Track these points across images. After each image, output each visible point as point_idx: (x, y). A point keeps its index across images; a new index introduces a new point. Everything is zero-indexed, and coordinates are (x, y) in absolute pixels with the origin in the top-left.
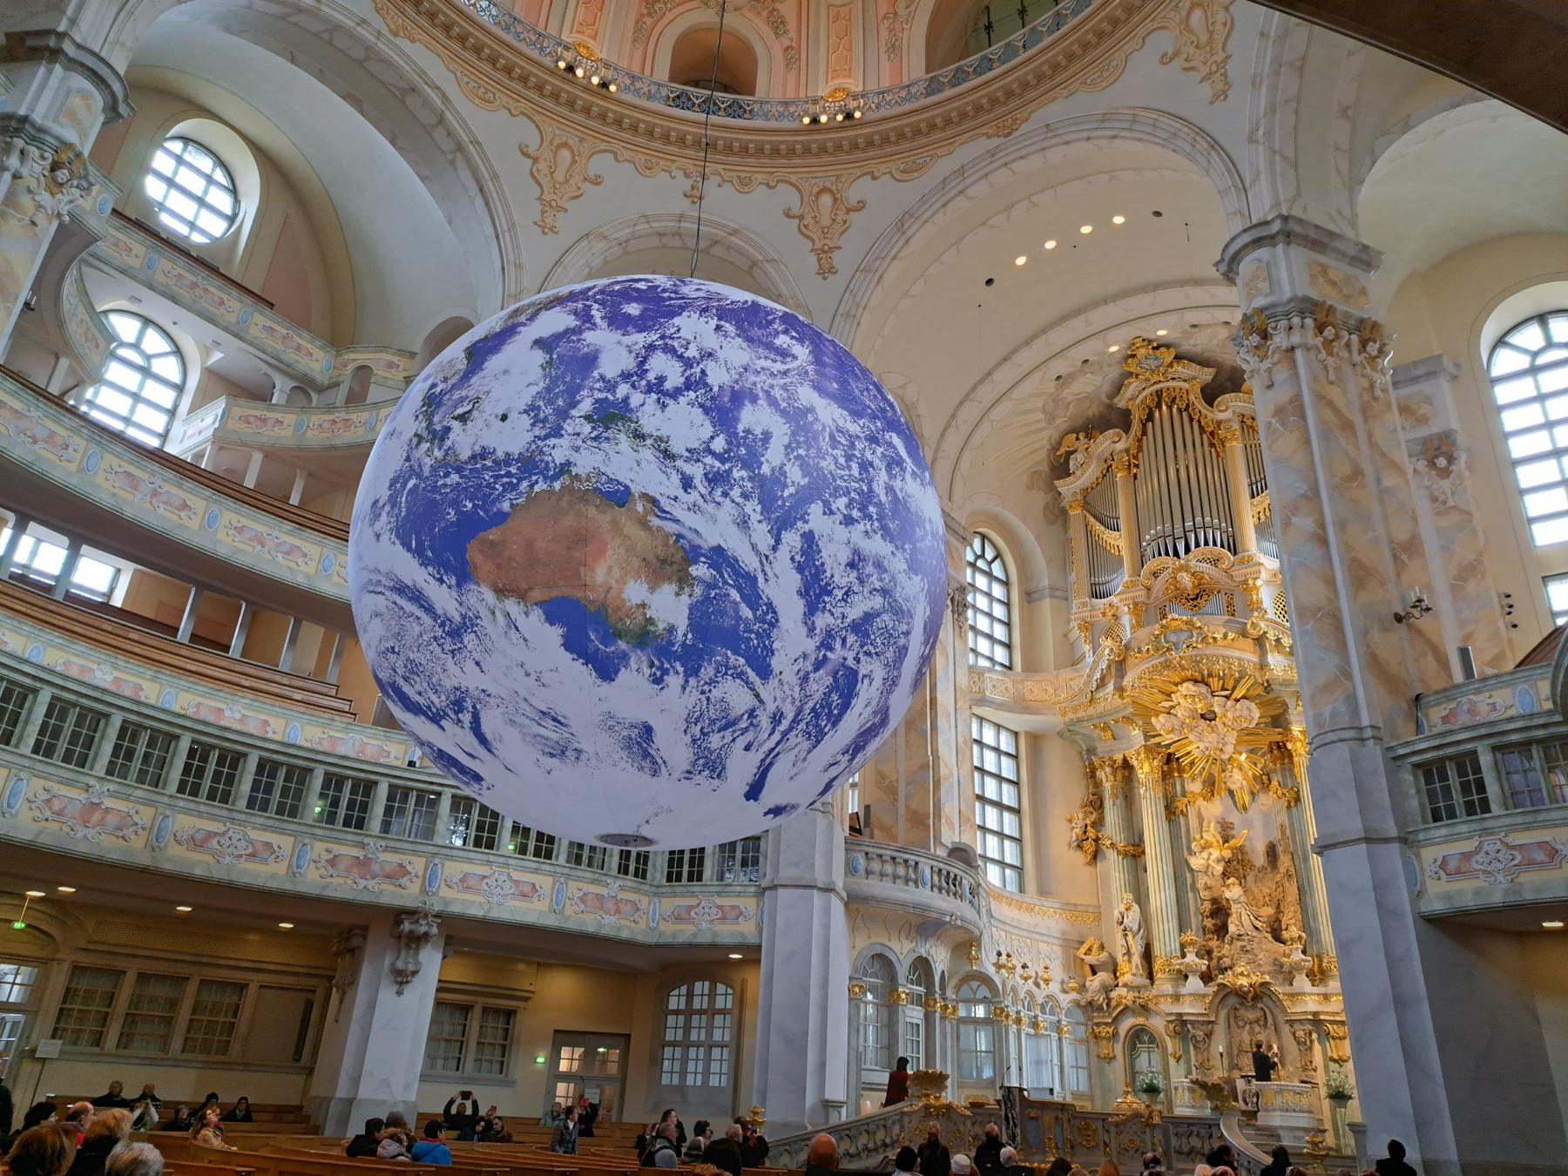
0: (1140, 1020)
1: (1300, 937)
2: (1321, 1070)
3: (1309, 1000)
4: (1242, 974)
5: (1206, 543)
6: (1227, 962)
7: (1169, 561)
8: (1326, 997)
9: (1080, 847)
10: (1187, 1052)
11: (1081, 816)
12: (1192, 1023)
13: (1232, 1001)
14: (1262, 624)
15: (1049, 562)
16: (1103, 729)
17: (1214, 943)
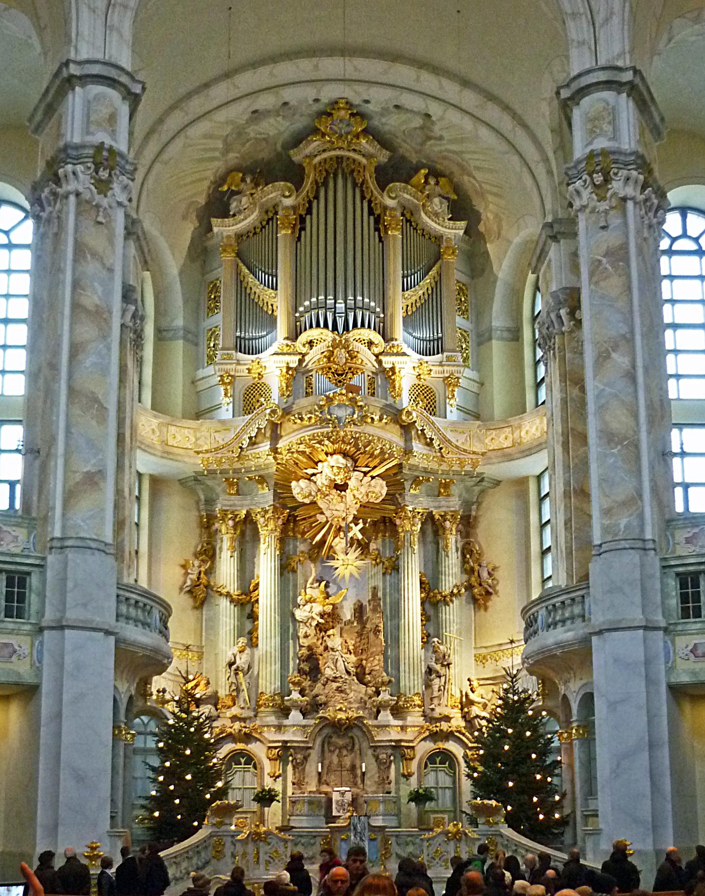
0: (240, 746)
1: (390, 681)
2: (393, 784)
3: (390, 729)
4: (340, 710)
5: (363, 325)
6: (322, 699)
7: (328, 335)
8: (403, 728)
9: (190, 592)
10: (285, 771)
11: (197, 563)
12: (294, 748)
13: (326, 731)
14: (414, 414)
15: (186, 302)
16: (231, 485)
17: (306, 683)
